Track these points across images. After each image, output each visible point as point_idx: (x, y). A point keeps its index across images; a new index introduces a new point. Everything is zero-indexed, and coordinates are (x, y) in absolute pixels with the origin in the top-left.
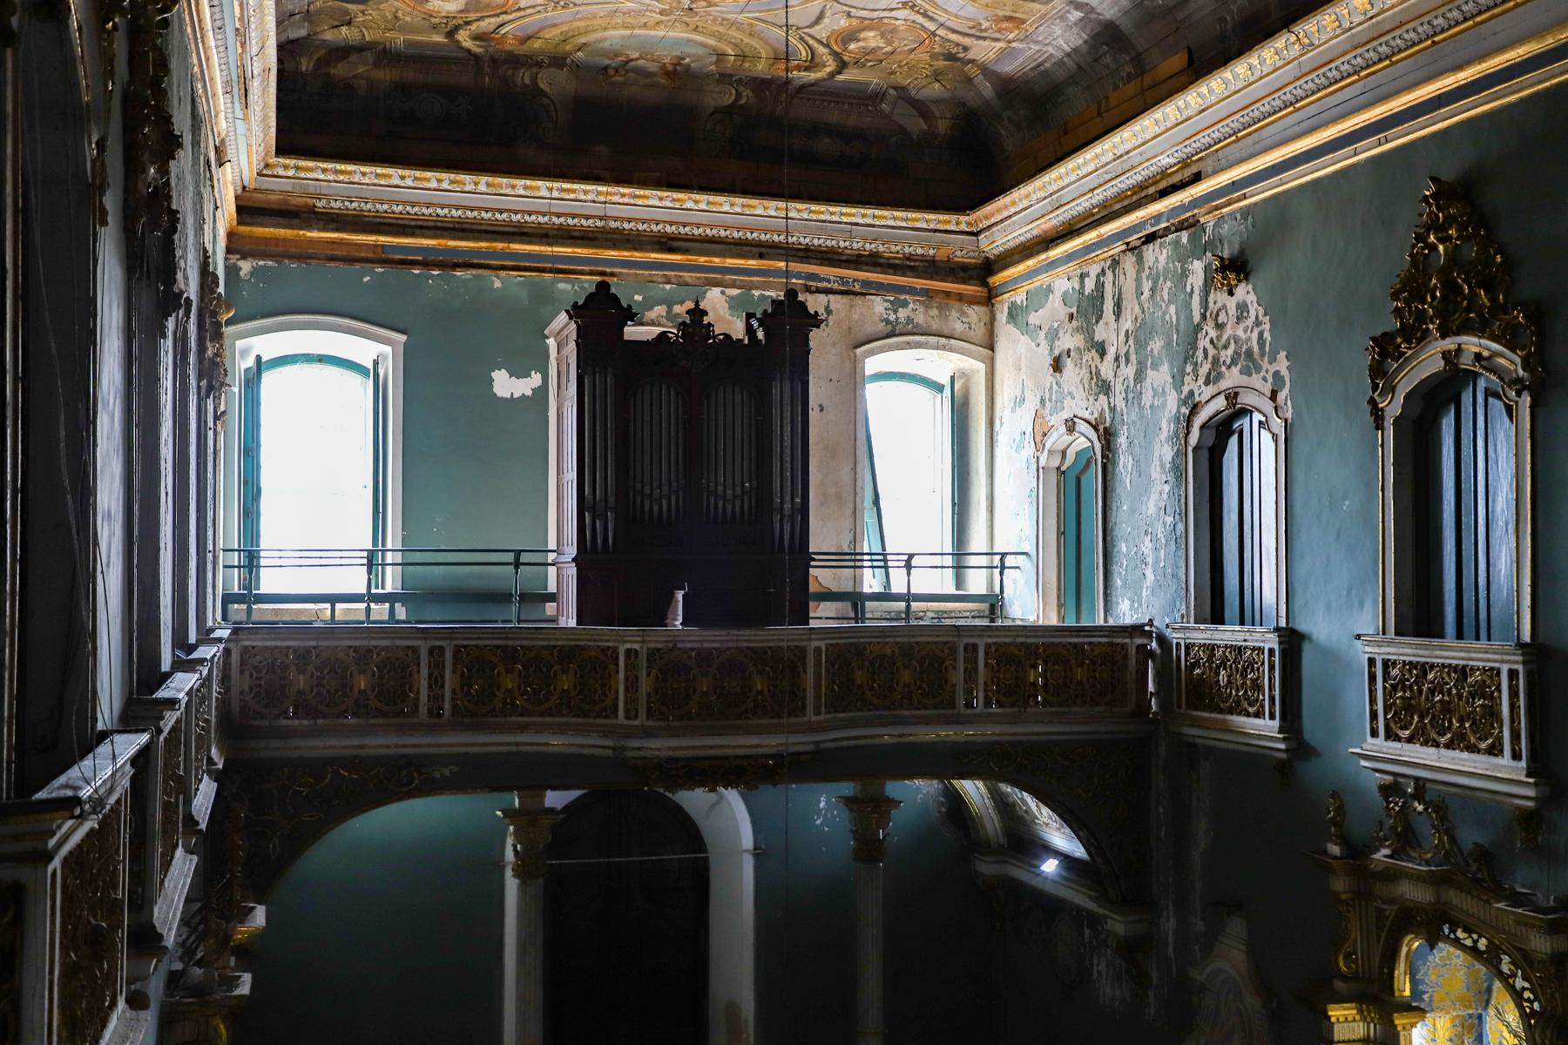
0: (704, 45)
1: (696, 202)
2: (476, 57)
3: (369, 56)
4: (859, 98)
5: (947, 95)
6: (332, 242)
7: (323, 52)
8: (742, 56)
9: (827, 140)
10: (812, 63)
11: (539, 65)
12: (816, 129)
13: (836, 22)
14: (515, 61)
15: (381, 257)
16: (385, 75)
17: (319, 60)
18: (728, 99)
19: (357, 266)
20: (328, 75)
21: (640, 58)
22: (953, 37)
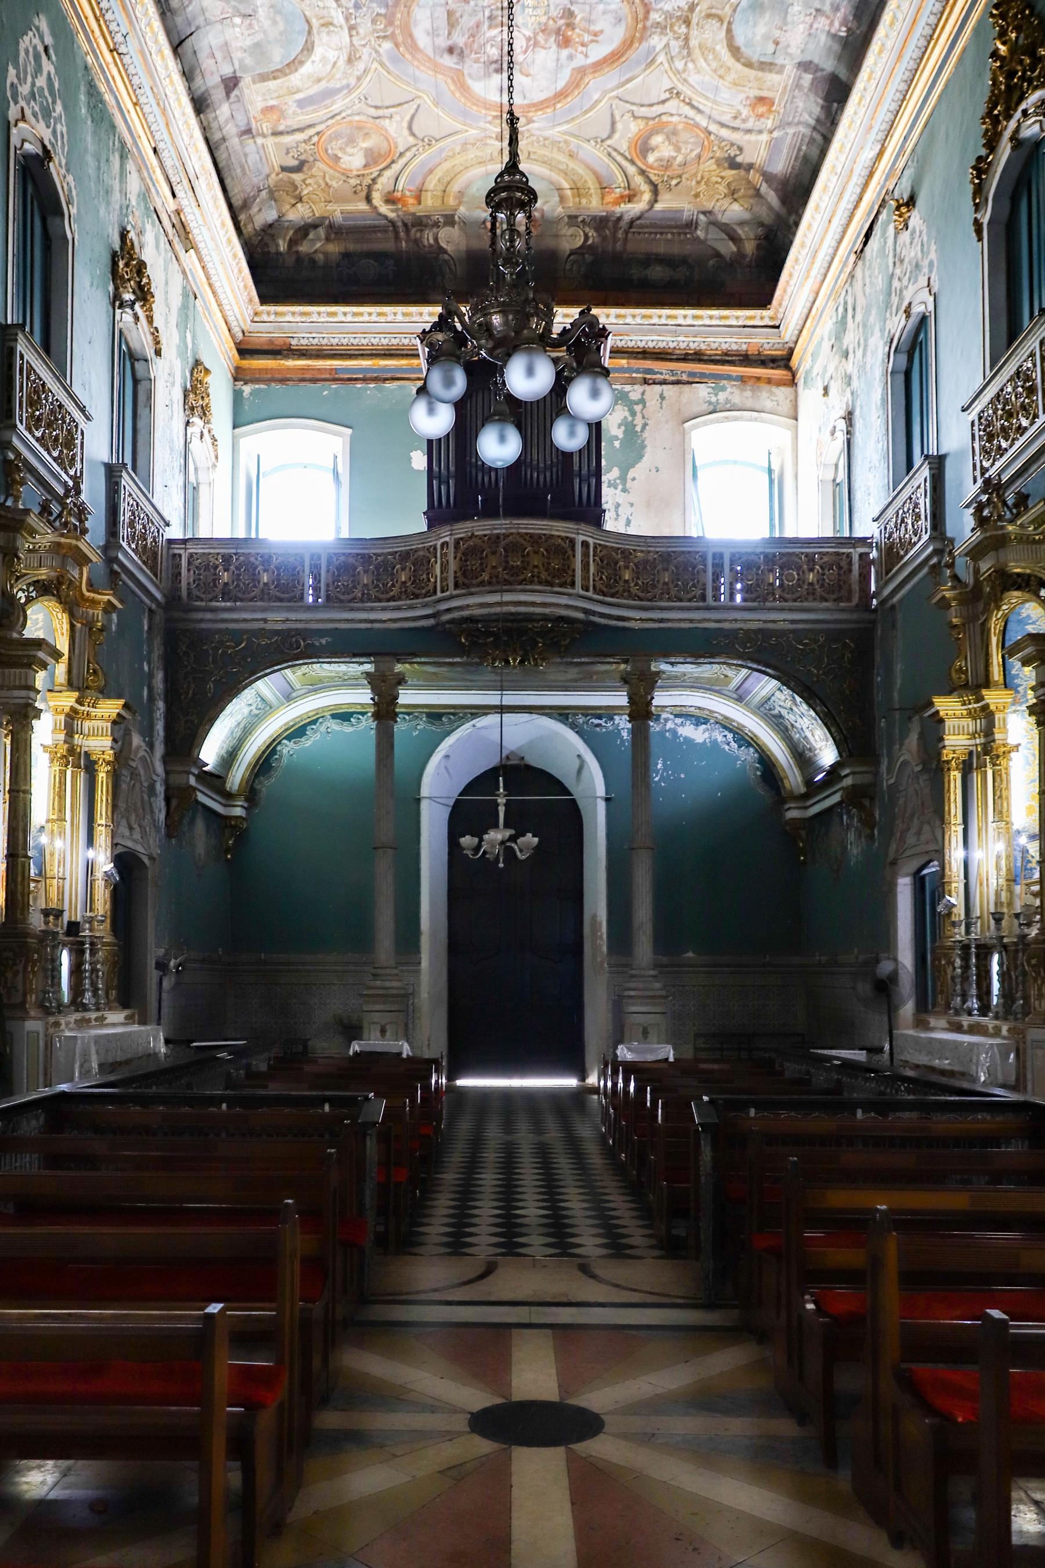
2: (392, 222)
3: (321, 231)
4: (676, 227)
5: (746, 216)
6: (302, 369)
7: (291, 233)
8: (578, 191)
9: (658, 268)
11: (436, 224)
12: (650, 260)
14: (420, 223)
15: (335, 377)
16: (334, 248)
17: (290, 239)
18: (579, 242)
19: (319, 385)
20: (297, 252)
22: (724, 133)
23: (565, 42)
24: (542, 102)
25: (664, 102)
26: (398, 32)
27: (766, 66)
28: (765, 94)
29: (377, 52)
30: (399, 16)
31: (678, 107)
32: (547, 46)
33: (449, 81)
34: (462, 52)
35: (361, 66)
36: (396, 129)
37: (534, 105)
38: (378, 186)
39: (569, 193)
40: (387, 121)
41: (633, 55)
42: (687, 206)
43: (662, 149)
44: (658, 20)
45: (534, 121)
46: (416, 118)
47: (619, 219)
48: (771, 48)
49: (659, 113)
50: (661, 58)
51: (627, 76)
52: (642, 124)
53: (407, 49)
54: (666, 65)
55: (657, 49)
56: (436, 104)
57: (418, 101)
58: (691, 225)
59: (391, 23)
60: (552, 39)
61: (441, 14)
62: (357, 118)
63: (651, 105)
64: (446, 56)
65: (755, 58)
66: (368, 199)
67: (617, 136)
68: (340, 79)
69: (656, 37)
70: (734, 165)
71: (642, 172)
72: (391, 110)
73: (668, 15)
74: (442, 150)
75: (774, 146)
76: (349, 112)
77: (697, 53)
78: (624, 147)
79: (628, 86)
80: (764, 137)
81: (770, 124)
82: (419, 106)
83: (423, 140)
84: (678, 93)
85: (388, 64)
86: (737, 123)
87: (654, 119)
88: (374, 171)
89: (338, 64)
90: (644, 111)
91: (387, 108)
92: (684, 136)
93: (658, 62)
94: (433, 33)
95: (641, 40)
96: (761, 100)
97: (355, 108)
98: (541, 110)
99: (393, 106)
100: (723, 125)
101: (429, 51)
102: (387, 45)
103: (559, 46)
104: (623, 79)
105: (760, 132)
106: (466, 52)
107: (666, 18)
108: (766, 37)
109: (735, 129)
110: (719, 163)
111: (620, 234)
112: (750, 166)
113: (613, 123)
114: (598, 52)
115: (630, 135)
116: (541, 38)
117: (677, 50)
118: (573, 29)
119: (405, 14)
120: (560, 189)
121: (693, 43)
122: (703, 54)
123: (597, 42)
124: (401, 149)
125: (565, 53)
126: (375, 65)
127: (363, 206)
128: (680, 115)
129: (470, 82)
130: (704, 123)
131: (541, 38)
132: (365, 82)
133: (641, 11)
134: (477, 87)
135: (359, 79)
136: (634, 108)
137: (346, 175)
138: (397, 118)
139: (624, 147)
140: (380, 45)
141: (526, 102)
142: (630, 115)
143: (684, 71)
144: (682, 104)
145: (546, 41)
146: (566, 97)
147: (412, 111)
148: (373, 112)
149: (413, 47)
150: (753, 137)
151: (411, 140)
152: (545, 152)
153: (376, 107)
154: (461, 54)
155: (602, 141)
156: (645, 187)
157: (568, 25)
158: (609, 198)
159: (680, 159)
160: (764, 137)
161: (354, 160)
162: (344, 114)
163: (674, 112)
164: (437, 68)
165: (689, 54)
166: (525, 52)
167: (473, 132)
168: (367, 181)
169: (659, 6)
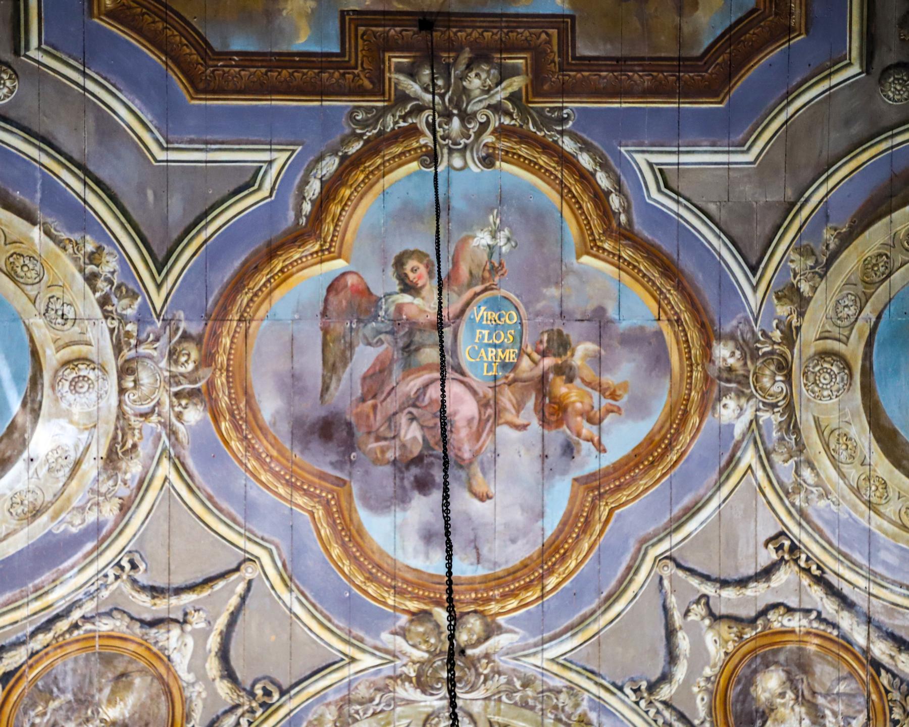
24: (513, 573)
25: (767, 573)
26: (221, 381)
29: (172, 433)
30: (226, 341)
31: (800, 589)
32: (520, 421)
33: (320, 513)
34: (351, 434)
35: (134, 469)
37: (496, 580)
40: (175, 631)
41: (693, 444)
44: (731, 361)
45: (499, 630)
46: (240, 619)
49: (761, 606)
50: (749, 457)
51: (687, 500)
53: (237, 428)
54: (760, 473)
55: (738, 432)
57: (249, 572)
59: (207, 359)
60: (531, 403)
61: (311, 335)
62: (105, 626)
63: (742, 583)
64: (316, 445)
67: (680, 672)
68: (81, 509)
69: (731, 402)
72: (187, 598)
76: (88, 608)
79: (692, 526)
82: (250, 582)
83: (252, 694)
84: (794, 548)
85: (190, 463)
87: (752, 622)
89: (84, 466)
90: (728, 599)
91: (178, 591)
92: (825, 673)
93: (743, 466)
94: (292, 384)
97: (105, 593)
98: (513, 594)
99: (191, 588)
102: (194, 415)
103: (544, 422)
104: (677, 509)
106: (360, 433)
107: (744, 357)
113: (670, 633)
114: (623, 437)
115: (708, 671)
116: (507, 398)
117: (775, 435)
118: (570, 380)
119: (240, 337)
122: (826, 446)
123: (618, 410)
125: (557, 437)
126: (166, 469)
128: (808, 611)
129: (364, 515)
130: (859, 636)
133: (693, 334)
134: (378, 527)
136: (708, 589)
138: (198, 622)
140: (179, 416)
141: (481, 571)
142: (699, 610)
143: (798, 488)
144: (806, 581)
145: (519, 407)
146: (564, 558)
147: (234, 601)
148: (144, 605)
149: (247, 420)
151: (223, 688)
153: (155, 591)
154: (349, 444)
155: (652, 687)
157: (559, 370)
162: (76, 615)
163: (793, 603)
165: (801, 447)
166: (478, 435)
167: (366, 661)
169: (727, 328)
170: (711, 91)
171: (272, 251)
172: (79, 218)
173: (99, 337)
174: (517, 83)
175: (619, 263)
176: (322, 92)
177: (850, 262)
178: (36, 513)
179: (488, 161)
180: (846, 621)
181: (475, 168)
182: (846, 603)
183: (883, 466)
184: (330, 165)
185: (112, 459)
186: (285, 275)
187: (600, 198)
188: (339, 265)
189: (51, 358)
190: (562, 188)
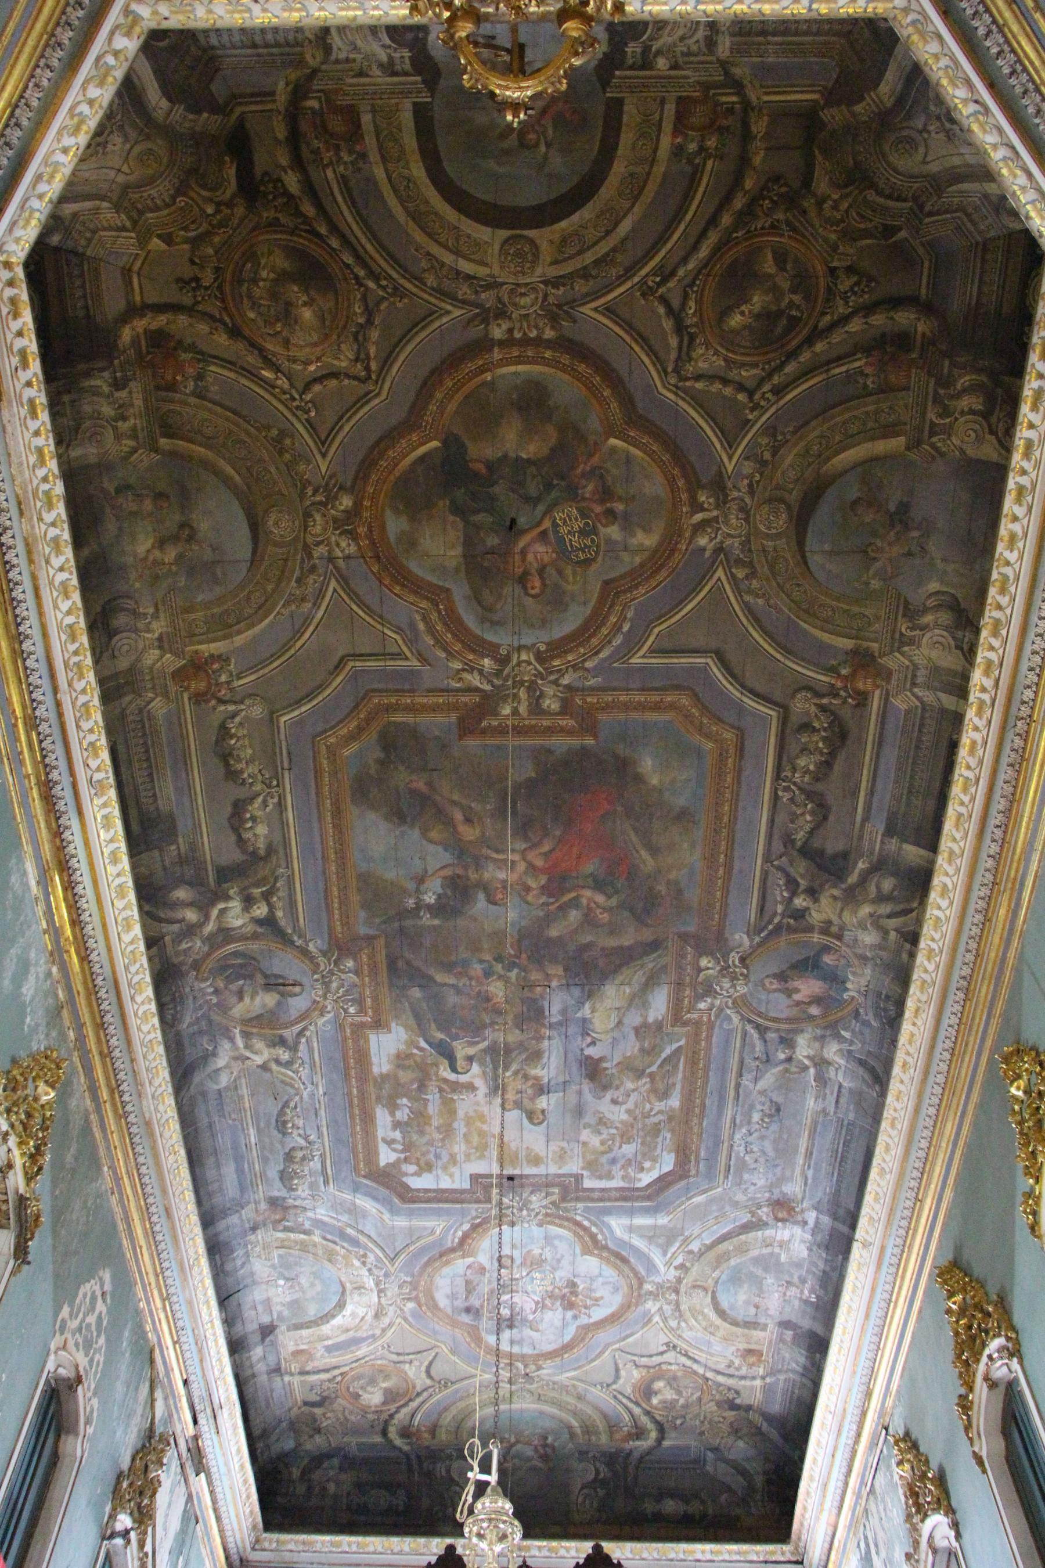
0: (553, 1417)
1: (567, 1549)
2: (407, 1455)
3: (336, 1462)
10: (639, 1433)
11: (449, 1457)
13: (631, 1377)
18: (591, 1476)
21: (517, 1442)
22: (720, 1379)
23: (570, 1306)
25: (662, 1353)
27: (751, 1325)
28: (753, 1347)
35: (386, 1321)
36: (415, 1373)
38: (395, 1421)
39: (579, 1431)
41: (632, 1315)
42: (693, 1443)
43: (663, 1393)
47: (630, 1453)
48: (753, 1311)
50: (657, 1318)
52: (644, 1372)
56: (453, 1352)
58: (699, 1462)
61: (460, 1283)
65: (740, 1318)
66: (384, 1433)
70: (733, 1406)
71: (648, 1413)
73: (659, 1286)
74: (457, 1391)
75: (768, 1390)
77: (688, 1314)
78: (628, 1391)
80: (758, 1383)
81: (761, 1372)
86: (731, 1371)
88: (393, 1408)
90: (644, 1361)
94: (453, 1296)
95: (637, 1305)
96: (750, 1352)
100: (718, 1372)
101: (449, 1311)
102: (411, 1305)
103: (565, 1309)
105: (754, 1378)
108: (747, 1302)
109: (731, 1376)
110: (719, 1404)
111: (631, 1469)
112: (749, 1408)
113: (617, 1370)
116: (548, 1302)
120: (570, 1428)
121: (684, 1307)
124: (419, 1389)
125: (570, 1314)
127: (378, 1439)
130: (701, 1371)
131: (548, 1302)
132: (389, 1333)
133: (635, 1282)
135: (384, 1330)
137: (365, 1411)
138: (416, 1363)
139: (628, 1391)
148: (394, 1358)
149: (435, 1307)
150: (748, 1383)
151: (429, 1382)
152: (552, 1394)
156: (650, 1425)
158: (617, 1436)
159: (682, 1401)
160: (758, 1383)
161: (373, 1398)
164: (455, 1324)
168: (385, 1416)
170: (649, 1198)
171: (441, 1255)
172: (355, 1242)
173: (370, 1283)
174: (555, 1198)
175: (601, 1257)
176: (462, 1202)
177: (711, 1255)
178: (348, 1330)
179: (540, 1225)
180: (695, 1367)
181: (535, 1228)
182: (696, 1361)
183: (718, 1321)
184: (466, 1227)
185: (377, 1316)
186: (447, 1263)
187: (593, 1237)
188: (470, 1260)
189: (348, 1286)
190: (575, 1233)
